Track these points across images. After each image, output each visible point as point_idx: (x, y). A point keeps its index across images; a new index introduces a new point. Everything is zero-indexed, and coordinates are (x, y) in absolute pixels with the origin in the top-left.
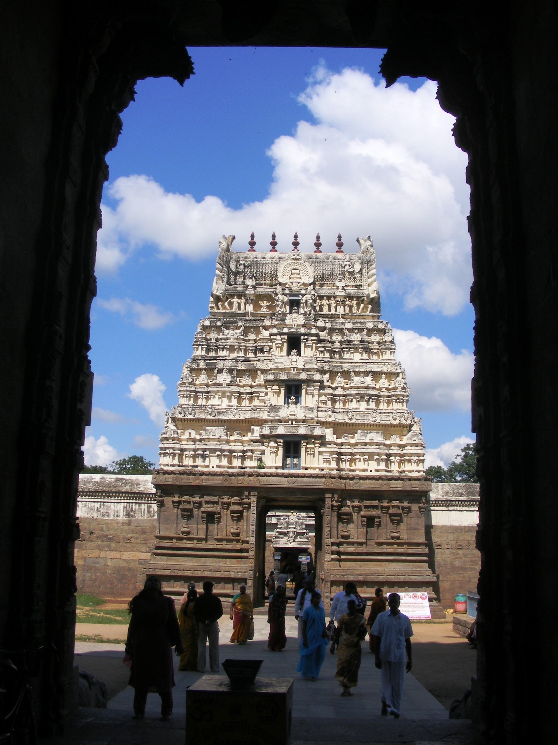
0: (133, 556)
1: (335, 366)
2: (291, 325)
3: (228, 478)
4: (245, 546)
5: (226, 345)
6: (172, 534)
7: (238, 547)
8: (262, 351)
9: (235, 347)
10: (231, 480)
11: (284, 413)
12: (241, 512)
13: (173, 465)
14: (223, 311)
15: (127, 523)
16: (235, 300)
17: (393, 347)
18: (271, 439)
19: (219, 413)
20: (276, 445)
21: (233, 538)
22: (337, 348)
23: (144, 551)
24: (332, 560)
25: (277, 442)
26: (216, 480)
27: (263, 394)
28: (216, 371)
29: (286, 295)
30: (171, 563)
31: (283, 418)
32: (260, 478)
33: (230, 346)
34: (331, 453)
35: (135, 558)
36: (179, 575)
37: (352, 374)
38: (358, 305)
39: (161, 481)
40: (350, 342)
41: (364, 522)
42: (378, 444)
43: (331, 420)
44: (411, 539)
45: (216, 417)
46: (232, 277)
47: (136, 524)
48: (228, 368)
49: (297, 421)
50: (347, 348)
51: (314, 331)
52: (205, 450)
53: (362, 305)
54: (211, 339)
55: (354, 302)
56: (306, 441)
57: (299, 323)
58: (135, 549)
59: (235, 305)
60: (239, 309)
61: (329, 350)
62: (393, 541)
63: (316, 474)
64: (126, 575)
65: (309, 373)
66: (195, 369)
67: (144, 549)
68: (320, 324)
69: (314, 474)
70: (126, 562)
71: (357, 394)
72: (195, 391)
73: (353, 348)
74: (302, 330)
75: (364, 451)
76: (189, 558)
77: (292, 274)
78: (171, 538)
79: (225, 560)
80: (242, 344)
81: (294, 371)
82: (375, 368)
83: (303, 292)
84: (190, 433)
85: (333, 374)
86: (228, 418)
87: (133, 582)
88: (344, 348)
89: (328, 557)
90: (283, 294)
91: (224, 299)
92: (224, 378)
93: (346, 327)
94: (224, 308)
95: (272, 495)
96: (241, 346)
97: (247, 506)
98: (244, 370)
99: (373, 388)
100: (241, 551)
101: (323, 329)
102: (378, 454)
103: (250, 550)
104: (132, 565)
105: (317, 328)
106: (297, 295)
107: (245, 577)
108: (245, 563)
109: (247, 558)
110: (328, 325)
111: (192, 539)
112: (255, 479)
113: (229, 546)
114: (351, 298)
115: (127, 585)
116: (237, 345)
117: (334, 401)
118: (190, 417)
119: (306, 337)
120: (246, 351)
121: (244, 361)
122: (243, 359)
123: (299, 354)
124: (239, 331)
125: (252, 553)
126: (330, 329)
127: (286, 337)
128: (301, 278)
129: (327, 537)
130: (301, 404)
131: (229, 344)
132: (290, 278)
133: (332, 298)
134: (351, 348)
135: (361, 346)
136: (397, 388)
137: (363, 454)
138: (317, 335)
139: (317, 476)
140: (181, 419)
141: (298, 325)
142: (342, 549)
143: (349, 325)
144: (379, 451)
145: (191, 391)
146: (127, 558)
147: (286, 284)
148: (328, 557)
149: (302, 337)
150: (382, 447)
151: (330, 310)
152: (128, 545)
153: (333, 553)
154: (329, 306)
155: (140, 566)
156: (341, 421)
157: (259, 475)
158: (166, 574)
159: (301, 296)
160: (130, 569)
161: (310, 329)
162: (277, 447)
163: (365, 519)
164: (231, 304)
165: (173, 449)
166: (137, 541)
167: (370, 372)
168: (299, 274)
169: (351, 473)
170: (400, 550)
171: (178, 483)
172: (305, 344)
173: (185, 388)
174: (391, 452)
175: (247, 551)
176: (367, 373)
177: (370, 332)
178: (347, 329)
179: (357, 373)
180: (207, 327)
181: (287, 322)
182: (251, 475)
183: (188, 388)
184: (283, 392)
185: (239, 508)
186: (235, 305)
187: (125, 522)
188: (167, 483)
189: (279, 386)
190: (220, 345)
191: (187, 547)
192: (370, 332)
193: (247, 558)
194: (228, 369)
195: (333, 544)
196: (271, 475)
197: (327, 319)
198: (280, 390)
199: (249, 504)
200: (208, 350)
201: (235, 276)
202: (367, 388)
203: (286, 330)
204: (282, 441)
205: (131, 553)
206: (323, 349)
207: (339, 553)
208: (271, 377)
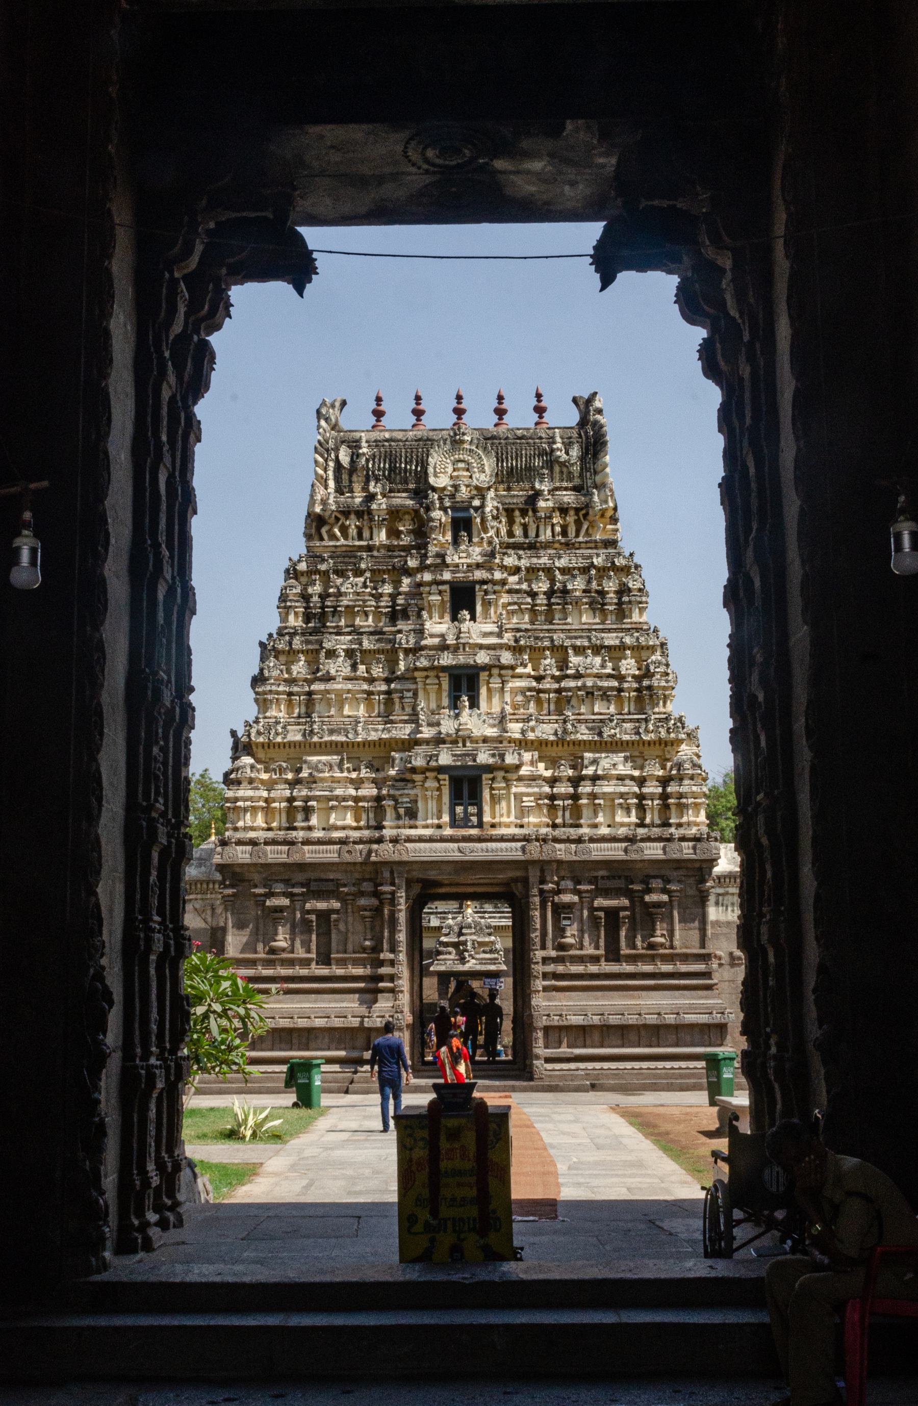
1: (537, 638)
2: (457, 566)
5: (339, 606)
8: (405, 614)
9: (356, 609)
11: (448, 726)
12: (378, 910)
13: (252, 829)
14: (331, 543)
17: (644, 599)
18: (428, 774)
19: (331, 732)
20: (436, 785)
22: (541, 605)
24: (545, 989)
25: (438, 780)
27: (410, 694)
28: (323, 654)
29: (444, 509)
31: (448, 735)
33: (347, 607)
34: (540, 797)
37: (570, 651)
38: (578, 524)
40: (565, 592)
42: (621, 778)
43: (531, 736)
44: (687, 948)
45: (327, 738)
46: (345, 477)
48: (344, 647)
49: (474, 741)
50: (558, 604)
51: (498, 575)
52: (307, 799)
53: (585, 527)
54: (311, 596)
55: (571, 519)
56: (491, 776)
57: (469, 561)
59: (353, 531)
60: (360, 537)
61: (526, 609)
65: (492, 652)
66: (283, 652)
68: (510, 561)
71: (579, 689)
72: (284, 693)
73: (571, 604)
74: (479, 575)
75: (597, 790)
77: (454, 470)
80: (369, 603)
81: (464, 649)
82: (611, 640)
83: (476, 503)
85: (536, 653)
88: (554, 604)
89: (539, 984)
90: (440, 509)
91: (332, 520)
92: (338, 667)
93: (557, 564)
94: (333, 537)
95: (432, 875)
96: (367, 607)
97: (389, 896)
98: (374, 651)
99: (609, 676)
101: (516, 570)
102: (622, 795)
105: (503, 568)
106: (466, 509)
110: (524, 563)
114: (563, 510)
116: (359, 606)
117: (539, 702)
118: (279, 739)
119: (485, 587)
120: (378, 614)
121: (371, 633)
122: (371, 629)
123: (473, 618)
124: (362, 579)
126: (528, 570)
127: (446, 587)
128: (471, 477)
130: (479, 709)
131: (345, 603)
132: (451, 477)
133: (530, 513)
134: (566, 604)
135: (584, 600)
136: (653, 675)
137: (593, 796)
138: (504, 582)
139: (513, 839)
140: (263, 745)
141: (469, 566)
142: (560, 969)
143: (562, 563)
144: (623, 789)
145: (278, 693)
147: (444, 489)
149: (477, 587)
150: (628, 782)
151: (526, 535)
153: (545, 976)
154: (525, 527)
156: (552, 738)
157: (409, 840)
159: (472, 511)
161: (490, 570)
164: (344, 530)
165: (250, 799)
167: (603, 647)
168: (468, 470)
169: (572, 830)
170: (667, 968)
171: (260, 861)
172: (483, 600)
173: (268, 688)
174: (645, 790)
176: (597, 650)
177: (603, 572)
178: (559, 569)
179: (579, 651)
180: (302, 573)
181: (448, 560)
182: (395, 841)
183: (274, 688)
184: (445, 685)
186: (353, 531)
189: (438, 677)
190: (328, 607)
192: (603, 572)
194: (344, 650)
195: (545, 960)
196: (431, 840)
197: (521, 552)
198: (440, 684)
200: (308, 618)
201: (350, 475)
202: (599, 676)
203: (447, 576)
204: (447, 777)
206: (516, 607)
207: (556, 976)
208: (423, 663)
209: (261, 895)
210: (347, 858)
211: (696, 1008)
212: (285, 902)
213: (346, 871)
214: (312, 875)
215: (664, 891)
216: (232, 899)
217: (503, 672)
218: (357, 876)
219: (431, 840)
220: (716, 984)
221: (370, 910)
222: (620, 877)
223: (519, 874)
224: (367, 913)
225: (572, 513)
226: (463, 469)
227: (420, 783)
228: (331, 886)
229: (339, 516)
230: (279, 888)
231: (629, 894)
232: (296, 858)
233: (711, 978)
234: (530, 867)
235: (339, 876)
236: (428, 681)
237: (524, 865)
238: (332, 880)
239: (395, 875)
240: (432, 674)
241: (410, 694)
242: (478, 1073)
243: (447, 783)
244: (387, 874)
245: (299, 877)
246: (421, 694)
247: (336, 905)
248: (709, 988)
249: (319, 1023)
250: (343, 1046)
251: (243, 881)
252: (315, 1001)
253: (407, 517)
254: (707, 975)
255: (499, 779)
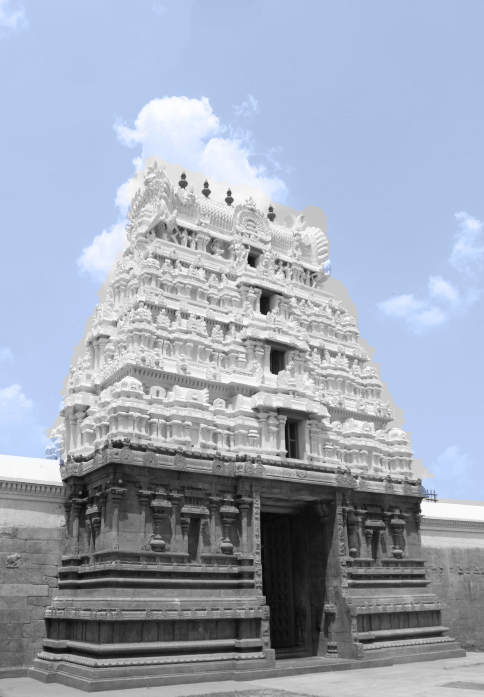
0: (18, 591)
3: (221, 463)
4: (246, 568)
6: (137, 550)
7: (236, 569)
10: (224, 466)
12: (237, 517)
15: (10, 534)
16: (184, 234)
20: (277, 423)
21: (224, 555)
23: (37, 582)
25: (278, 420)
26: (203, 465)
27: (244, 356)
30: (142, 599)
32: (264, 466)
35: (22, 595)
36: (160, 618)
39: (127, 459)
41: (370, 534)
44: (411, 557)
47: (26, 537)
55: (309, 276)
58: (23, 579)
62: (396, 559)
63: (324, 467)
64: (5, 624)
67: (36, 579)
69: (322, 467)
70: (7, 603)
76: (168, 590)
78: (135, 557)
79: (218, 591)
84: (158, 393)
86: (206, 379)
87: (16, 637)
97: (248, 506)
100: (239, 576)
103: (256, 575)
104: (16, 607)
107: (259, 616)
108: (250, 595)
109: (252, 586)
111: (168, 559)
112: (260, 467)
113: (223, 569)
115: (6, 642)
125: (258, 580)
129: (341, 553)
146: (9, 595)
148: (347, 582)
152: (11, 571)
155: (31, 607)
158: (139, 619)
160: (11, 614)
162: (278, 426)
163: (371, 531)
166: (25, 565)
168: (255, 227)
170: (407, 571)
171: (152, 465)
175: (251, 575)
185: (233, 510)
187: (7, 532)
188: (135, 463)
191: (180, 571)
193: (252, 586)
196: (275, 464)
199: (251, 504)
204: (285, 418)
205: (15, 585)
209: (147, 496)
210: (219, 472)
211: (425, 600)
212: (165, 503)
213: (211, 483)
214: (186, 483)
215: (400, 517)
216: (120, 497)
217: (301, 354)
218: (219, 488)
219: (275, 464)
220: (430, 583)
221: (230, 517)
222: (376, 506)
223: (325, 497)
224: (229, 520)
225: (309, 273)
226: (252, 226)
227: (265, 420)
228: (200, 495)
229: (177, 229)
230: (161, 492)
231: (383, 517)
232: (180, 467)
233: (424, 579)
234: (337, 493)
235: (206, 486)
236: (257, 349)
237: (332, 490)
238: (200, 489)
239: (254, 489)
240: (261, 344)
241: (244, 356)
242: (280, 655)
243: (285, 422)
244: (247, 488)
245: (176, 483)
246: (251, 356)
247: (207, 512)
248: (424, 585)
249: (201, 615)
250: (215, 636)
251: (129, 482)
252: (190, 595)
253: (218, 244)
254: (421, 576)
255: (314, 426)
